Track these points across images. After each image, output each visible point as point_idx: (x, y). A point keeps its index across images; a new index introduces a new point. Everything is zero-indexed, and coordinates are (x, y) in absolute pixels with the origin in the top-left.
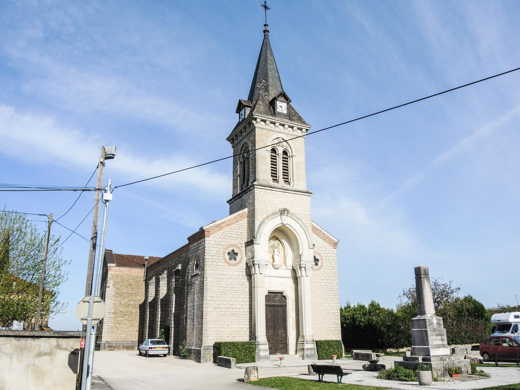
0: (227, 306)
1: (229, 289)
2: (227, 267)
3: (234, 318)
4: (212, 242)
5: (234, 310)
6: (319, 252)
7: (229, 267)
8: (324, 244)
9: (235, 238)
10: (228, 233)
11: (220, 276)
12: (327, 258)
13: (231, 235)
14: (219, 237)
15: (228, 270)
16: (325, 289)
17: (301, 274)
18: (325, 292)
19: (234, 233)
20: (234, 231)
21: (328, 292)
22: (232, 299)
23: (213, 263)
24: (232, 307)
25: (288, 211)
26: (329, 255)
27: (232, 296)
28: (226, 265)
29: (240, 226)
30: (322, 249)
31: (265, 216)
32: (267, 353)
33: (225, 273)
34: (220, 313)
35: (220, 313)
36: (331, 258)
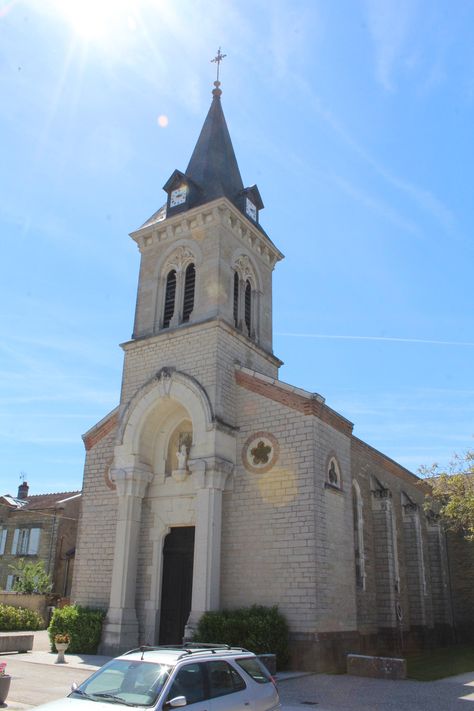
0: (104, 556)
6: (271, 430)
8: (282, 412)
12: (290, 439)
15: (109, 496)
21: (287, 515)
26: (293, 432)
30: (277, 423)
33: (105, 502)
34: (93, 568)
35: (93, 568)
36: (297, 438)
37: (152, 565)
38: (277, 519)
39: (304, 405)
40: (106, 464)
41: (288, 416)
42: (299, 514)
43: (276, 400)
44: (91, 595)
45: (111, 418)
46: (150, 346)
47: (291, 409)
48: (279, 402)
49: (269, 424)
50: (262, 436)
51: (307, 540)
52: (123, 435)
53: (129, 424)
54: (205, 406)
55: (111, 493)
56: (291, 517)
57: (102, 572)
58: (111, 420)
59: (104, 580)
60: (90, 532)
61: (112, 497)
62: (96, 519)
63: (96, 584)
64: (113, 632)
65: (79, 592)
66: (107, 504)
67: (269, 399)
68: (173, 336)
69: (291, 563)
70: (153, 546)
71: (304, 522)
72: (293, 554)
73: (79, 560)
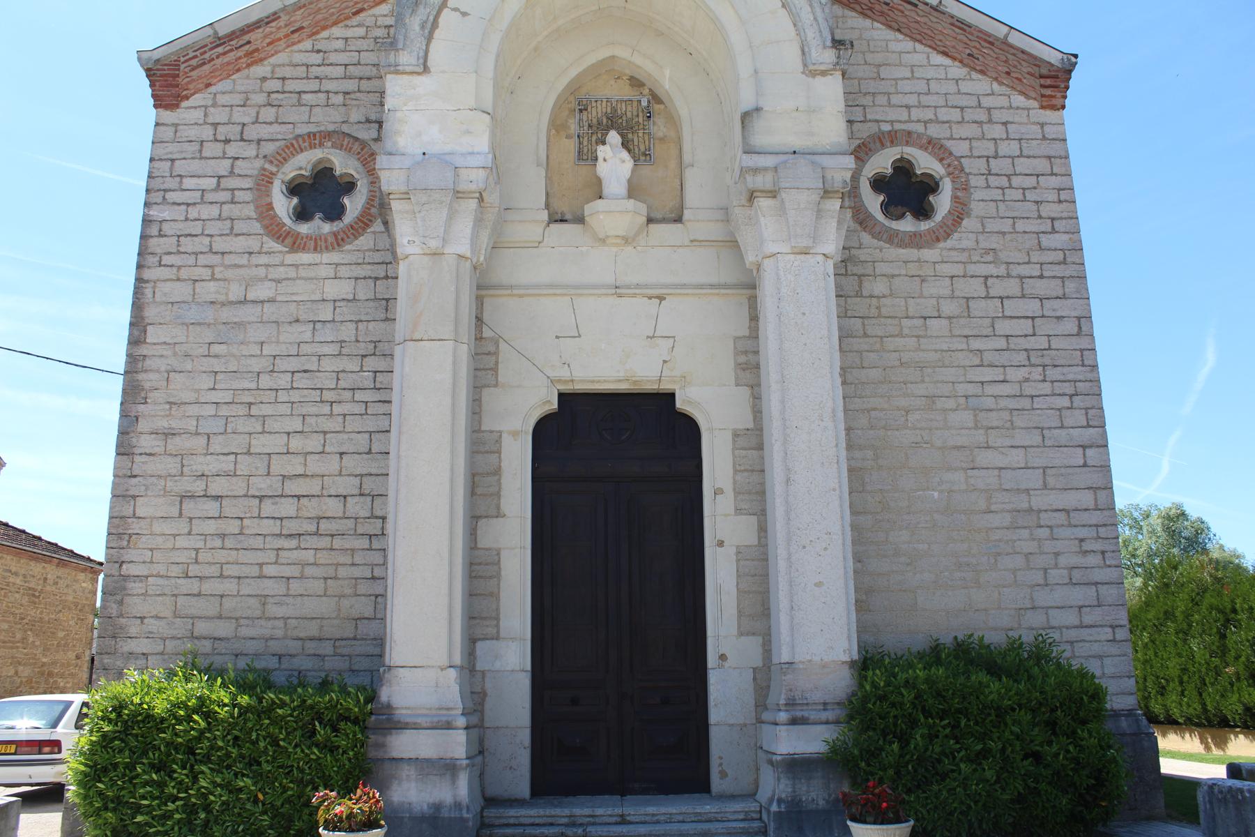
0: (261, 485)
2: (276, 259)
3: (309, 556)
4: (193, 133)
5: (311, 507)
6: (934, 131)
8: (966, 87)
9: (339, 99)
11: (226, 314)
14: (237, 99)
15: (280, 272)
16: (988, 357)
18: (989, 374)
21: (1014, 374)
22: (296, 443)
23: (188, 245)
24: (293, 487)
27: (297, 424)
30: (955, 115)
33: (262, 291)
34: (210, 527)
35: (210, 527)
36: (1023, 165)
37: (499, 515)
38: (982, 383)
39: (1043, 81)
41: (987, 102)
42: (1052, 373)
43: (945, 54)
44: (202, 628)
45: (284, 9)
47: (995, 85)
48: (954, 59)
49: (929, 114)
50: (907, 144)
51: (1084, 447)
52: (429, 38)
53: (456, 10)
56: (1027, 380)
58: (284, 18)
59: (270, 570)
60: (188, 396)
62: (216, 349)
63: (229, 587)
64: (427, 760)
65: (142, 618)
66: (272, 301)
67: (919, 47)
69: (1040, 511)
70: (499, 452)
71: (1071, 396)
72: (1045, 486)
73: (134, 497)
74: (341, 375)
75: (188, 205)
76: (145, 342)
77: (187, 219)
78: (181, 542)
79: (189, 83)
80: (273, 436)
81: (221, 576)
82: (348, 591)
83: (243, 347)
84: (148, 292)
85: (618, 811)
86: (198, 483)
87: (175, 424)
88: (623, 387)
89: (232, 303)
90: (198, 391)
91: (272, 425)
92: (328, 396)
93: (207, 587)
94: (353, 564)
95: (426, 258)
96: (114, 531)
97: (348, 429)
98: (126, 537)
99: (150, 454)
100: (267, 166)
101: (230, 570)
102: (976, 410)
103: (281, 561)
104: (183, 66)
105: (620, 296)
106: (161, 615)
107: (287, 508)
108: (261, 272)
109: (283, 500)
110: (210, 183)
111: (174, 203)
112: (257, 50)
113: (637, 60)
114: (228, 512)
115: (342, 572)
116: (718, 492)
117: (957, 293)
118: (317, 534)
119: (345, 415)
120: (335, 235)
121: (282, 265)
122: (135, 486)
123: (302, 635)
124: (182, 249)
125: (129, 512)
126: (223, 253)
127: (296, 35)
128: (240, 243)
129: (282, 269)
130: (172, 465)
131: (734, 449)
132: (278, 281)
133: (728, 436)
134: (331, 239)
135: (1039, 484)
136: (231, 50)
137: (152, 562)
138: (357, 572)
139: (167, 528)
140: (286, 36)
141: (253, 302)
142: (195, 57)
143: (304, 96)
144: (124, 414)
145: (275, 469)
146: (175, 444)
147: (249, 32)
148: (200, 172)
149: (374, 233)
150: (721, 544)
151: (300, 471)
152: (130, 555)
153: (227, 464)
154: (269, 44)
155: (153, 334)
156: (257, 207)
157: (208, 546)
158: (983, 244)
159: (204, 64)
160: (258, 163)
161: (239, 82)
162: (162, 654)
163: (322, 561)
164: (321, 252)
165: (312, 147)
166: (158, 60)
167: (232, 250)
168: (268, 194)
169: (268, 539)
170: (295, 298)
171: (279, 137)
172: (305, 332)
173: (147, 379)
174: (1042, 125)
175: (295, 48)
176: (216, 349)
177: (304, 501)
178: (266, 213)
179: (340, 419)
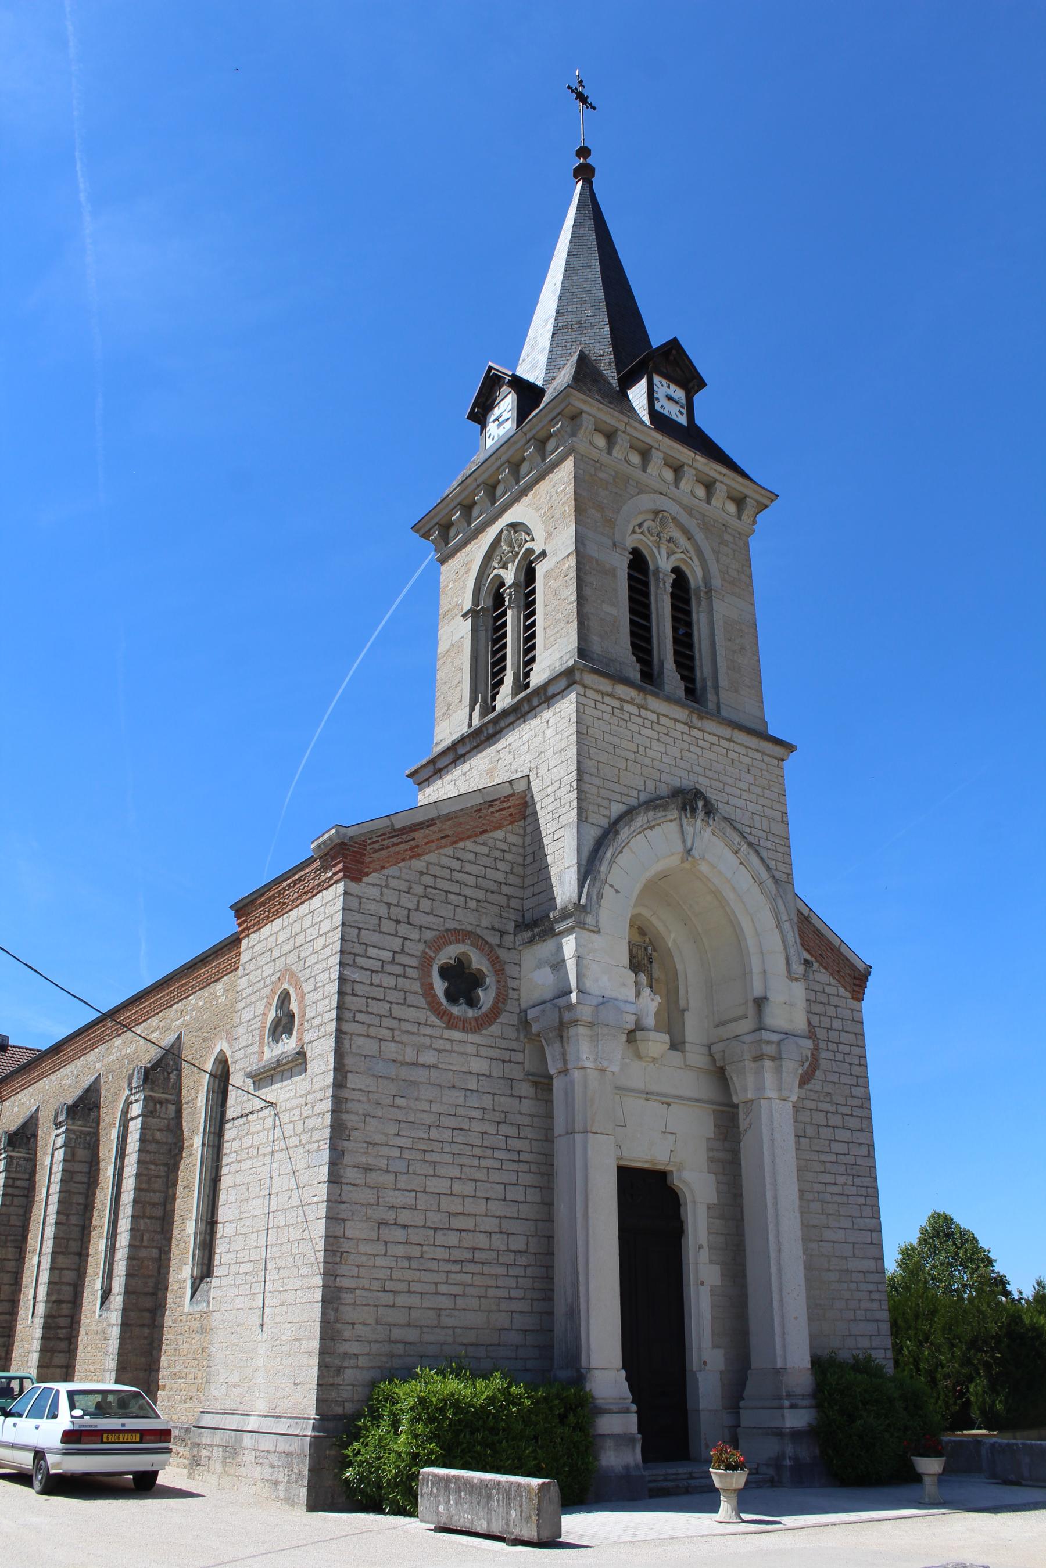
0: (434, 1219)
1: (447, 1135)
2: (437, 1032)
3: (467, 1278)
4: (372, 907)
5: (469, 1240)
7: (447, 1033)
9: (472, 904)
10: (446, 873)
11: (405, 1072)
12: (833, 1035)
13: (455, 888)
14: (403, 886)
15: (439, 1044)
16: (828, 1166)
17: (760, 1088)
18: (829, 1178)
19: (472, 880)
20: (469, 868)
21: (841, 1180)
22: (457, 1187)
23: (375, 1007)
24: (457, 1223)
25: (707, 803)
28: (433, 1019)
29: (498, 854)
31: (617, 809)
32: (633, 1456)
33: (428, 1058)
34: (400, 1250)
35: (400, 1250)
40: (421, 947)
42: (858, 1181)
44: (397, 1333)
45: (438, 817)
46: (644, 712)
51: (871, 1231)
53: (612, 886)
54: (787, 926)
55: (445, 1036)
56: (845, 1184)
57: (433, 1265)
58: (439, 825)
59: (443, 1289)
60: (379, 1138)
61: (449, 1048)
62: (399, 1101)
63: (415, 1301)
64: (618, 1435)
65: (353, 1324)
66: (435, 1067)
68: (699, 724)
71: (866, 1197)
73: (344, 1220)
74: (485, 1136)
75: (373, 971)
76: (345, 1087)
77: (372, 984)
78: (380, 1261)
79: (371, 862)
80: (441, 1180)
81: (409, 1292)
82: (494, 1308)
83: (417, 1103)
84: (346, 1042)
85: (690, 1470)
86: (390, 1213)
87: (371, 1161)
88: (646, 1166)
89: (407, 1063)
90: (387, 1135)
91: (441, 1171)
92: (477, 1151)
93: (401, 1300)
94: (497, 1287)
95: (596, 1072)
96: (329, 1248)
97: (491, 1180)
98: (339, 1254)
99: (354, 1185)
100: (427, 950)
101: (416, 1287)
102: (823, 1202)
103: (450, 1281)
104: (369, 847)
105: (647, 1099)
106: (368, 1322)
107: (453, 1239)
108: (428, 1041)
109: (450, 1232)
110: (387, 956)
111: (362, 968)
112: (417, 846)
113: (654, 920)
114: (414, 1239)
115: (491, 1292)
116: (701, 1247)
117: (814, 1122)
118: (473, 1261)
119: (488, 1169)
120: (476, 1019)
121: (441, 1038)
122: (344, 1211)
123: (465, 1341)
124: (370, 1010)
125: (341, 1234)
126: (400, 1020)
127: (443, 841)
128: (411, 1013)
129: (441, 1041)
130: (369, 1196)
131: (708, 1217)
132: (439, 1051)
133: (705, 1208)
134: (473, 1023)
135: (850, 1254)
136: (401, 843)
137: (358, 1277)
138: (501, 1293)
139: (368, 1248)
140: (438, 840)
141: (423, 1066)
142: (377, 842)
143: (450, 895)
144: (333, 1148)
145: (444, 1207)
146: (374, 1177)
147: (415, 830)
148: (380, 945)
149: (501, 1023)
150: (702, 1283)
151: (460, 1209)
152: (343, 1269)
153: (409, 1199)
154: (426, 844)
155: (352, 1081)
156: (422, 985)
157: (399, 1266)
158: (826, 1090)
159: (383, 849)
160: (421, 947)
161: (404, 870)
162: (368, 1354)
163: (476, 1283)
164: (467, 1032)
165: (457, 941)
166: (351, 838)
167: (406, 1018)
168: (430, 975)
169: (441, 1263)
170: (451, 1067)
171: (435, 927)
172: (458, 1097)
173: (351, 1120)
174: (853, 1010)
175: (442, 851)
176: (399, 1101)
177: (464, 1234)
178: (428, 990)
179: (485, 1171)
